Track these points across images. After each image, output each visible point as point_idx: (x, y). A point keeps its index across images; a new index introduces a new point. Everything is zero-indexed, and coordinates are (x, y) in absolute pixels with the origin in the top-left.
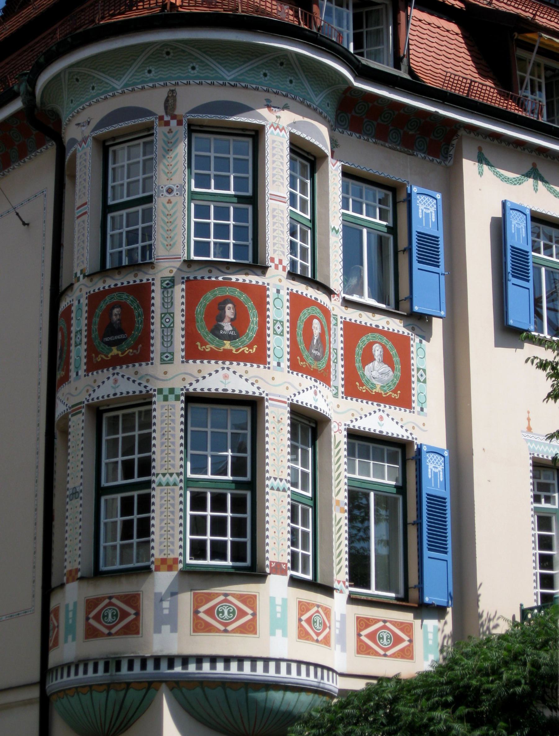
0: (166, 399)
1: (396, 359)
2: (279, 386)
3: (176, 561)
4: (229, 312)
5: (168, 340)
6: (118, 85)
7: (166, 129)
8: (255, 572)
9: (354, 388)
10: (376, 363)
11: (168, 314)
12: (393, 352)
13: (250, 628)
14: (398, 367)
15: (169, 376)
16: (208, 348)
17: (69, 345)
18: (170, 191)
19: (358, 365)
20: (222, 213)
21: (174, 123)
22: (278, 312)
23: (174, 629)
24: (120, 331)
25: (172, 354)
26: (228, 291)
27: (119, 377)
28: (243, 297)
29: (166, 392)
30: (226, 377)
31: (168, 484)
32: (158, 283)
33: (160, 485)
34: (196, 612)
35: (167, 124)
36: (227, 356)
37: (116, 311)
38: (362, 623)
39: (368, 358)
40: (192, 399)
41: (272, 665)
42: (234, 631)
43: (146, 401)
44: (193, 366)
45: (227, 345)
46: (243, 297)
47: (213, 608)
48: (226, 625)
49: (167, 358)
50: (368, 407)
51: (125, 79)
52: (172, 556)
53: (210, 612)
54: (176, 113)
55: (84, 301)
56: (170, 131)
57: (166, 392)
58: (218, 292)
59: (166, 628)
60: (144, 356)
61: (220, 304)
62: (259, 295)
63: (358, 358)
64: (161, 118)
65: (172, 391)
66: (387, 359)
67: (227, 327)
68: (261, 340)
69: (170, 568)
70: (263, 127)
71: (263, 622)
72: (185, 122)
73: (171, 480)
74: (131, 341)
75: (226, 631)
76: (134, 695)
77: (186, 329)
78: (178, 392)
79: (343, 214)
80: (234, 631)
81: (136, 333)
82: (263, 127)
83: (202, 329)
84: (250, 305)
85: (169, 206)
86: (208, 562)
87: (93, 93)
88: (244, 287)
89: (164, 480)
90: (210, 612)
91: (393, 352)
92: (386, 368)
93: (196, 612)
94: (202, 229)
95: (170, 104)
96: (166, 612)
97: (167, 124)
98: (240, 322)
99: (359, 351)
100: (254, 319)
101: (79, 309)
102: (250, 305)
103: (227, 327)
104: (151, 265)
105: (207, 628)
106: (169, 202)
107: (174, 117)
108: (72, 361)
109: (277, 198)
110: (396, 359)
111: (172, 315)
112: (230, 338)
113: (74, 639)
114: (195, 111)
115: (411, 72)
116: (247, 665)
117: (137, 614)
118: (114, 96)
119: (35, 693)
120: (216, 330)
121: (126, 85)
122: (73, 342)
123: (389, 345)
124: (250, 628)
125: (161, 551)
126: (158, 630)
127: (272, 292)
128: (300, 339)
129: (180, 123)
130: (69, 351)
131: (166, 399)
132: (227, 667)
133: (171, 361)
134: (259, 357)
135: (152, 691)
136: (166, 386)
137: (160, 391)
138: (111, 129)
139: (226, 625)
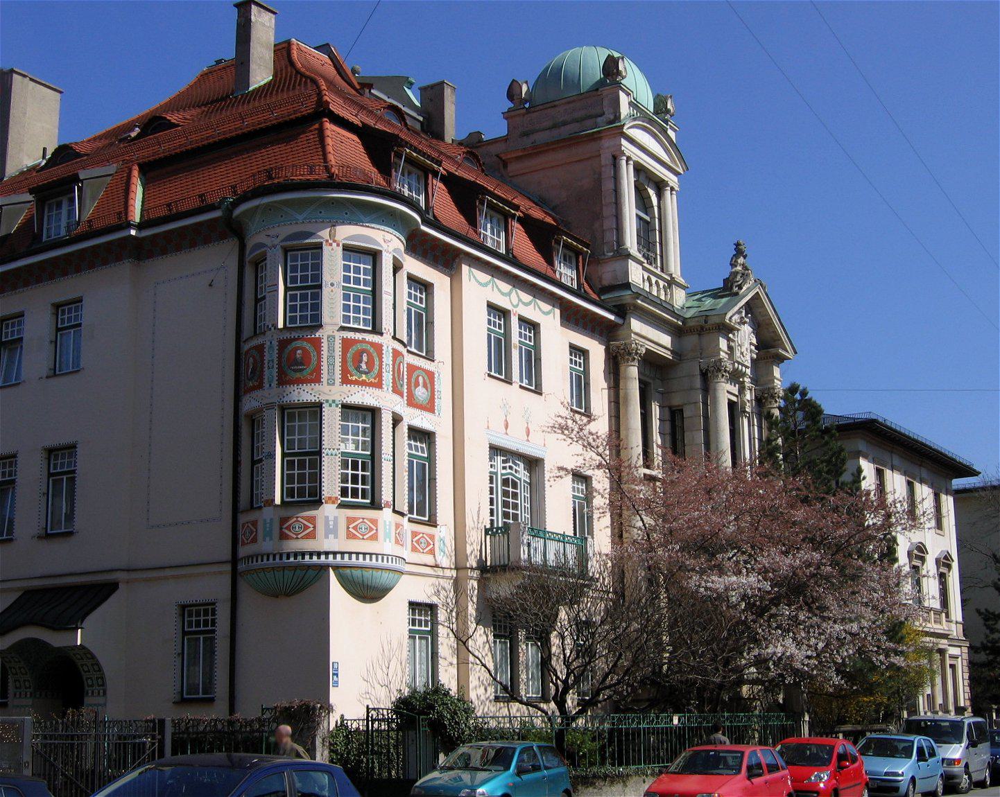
0: (330, 406)
1: (429, 385)
2: (386, 400)
3: (336, 498)
4: (365, 358)
5: (331, 372)
6: (300, 217)
7: (330, 248)
8: (375, 505)
9: (412, 402)
10: (420, 387)
11: (331, 357)
12: (428, 381)
13: (374, 538)
14: (429, 390)
15: (333, 392)
16: (354, 378)
17: (262, 367)
18: (332, 285)
19: (413, 388)
20: (357, 299)
21: (334, 245)
22: (388, 359)
23: (336, 537)
24: (302, 364)
25: (334, 380)
26: (364, 346)
27: (301, 391)
28: (372, 350)
29: (330, 402)
30: (363, 395)
31: (332, 455)
32: (325, 338)
33: (327, 455)
34: (348, 528)
35: (331, 245)
36: (363, 383)
37: (299, 352)
38: (414, 534)
39: (417, 384)
40: (345, 407)
41: (368, 556)
42: (367, 539)
43: (319, 406)
44: (346, 388)
45: (364, 377)
46: (372, 350)
47: (357, 525)
48: (363, 535)
49: (331, 383)
50: (417, 412)
51: (305, 215)
52: (334, 496)
53: (355, 528)
54: (336, 239)
55: (275, 343)
56: (332, 249)
57: (330, 402)
58: (359, 346)
59: (331, 536)
60: (318, 380)
61: (359, 355)
62: (378, 348)
63: (413, 385)
64: (327, 241)
65: (334, 401)
66: (425, 386)
67: (364, 366)
68: (380, 375)
69: (333, 503)
70: (381, 251)
71: (381, 534)
72: (341, 245)
73: (334, 452)
74: (308, 370)
75: (363, 539)
76: (311, 573)
77: (342, 366)
78: (337, 402)
79: (408, 302)
80: (367, 539)
81: (312, 366)
82: (381, 251)
83: (351, 368)
84: (375, 354)
85: (332, 294)
86: (349, 499)
87: (282, 219)
88: (372, 344)
89: (330, 452)
90: (355, 528)
91: (428, 381)
92: (424, 390)
93: (348, 528)
94: (346, 308)
95: (332, 235)
96: (331, 527)
97: (331, 245)
98: (370, 364)
99: (413, 380)
100: (377, 363)
101: (271, 347)
102: (375, 354)
103: (364, 366)
104: (321, 326)
105: (354, 537)
106: (332, 291)
107: (335, 241)
108: (266, 377)
109: (387, 293)
110: (429, 385)
111: (333, 357)
112: (366, 373)
113: (271, 539)
114: (345, 239)
115: (434, 216)
116: (339, 556)
117: (314, 527)
118: (297, 223)
119: (228, 568)
120: (358, 368)
121: (305, 218)
122: (266, 365)
123: (426, 378)
124: (374, 538)
125: (328, 493)
126: (327, 537)
127: (384, 348)
128: (396, 375)
129: (338, 245)
130: (262, 371)
131: (330, 406)
132: (327, 558)
133: (334, 384)
134: (379, 385)
135: (323, 571)
136: (331, 399)
137: (327, 401)
138: (295, 243)
139: (363, 535)
